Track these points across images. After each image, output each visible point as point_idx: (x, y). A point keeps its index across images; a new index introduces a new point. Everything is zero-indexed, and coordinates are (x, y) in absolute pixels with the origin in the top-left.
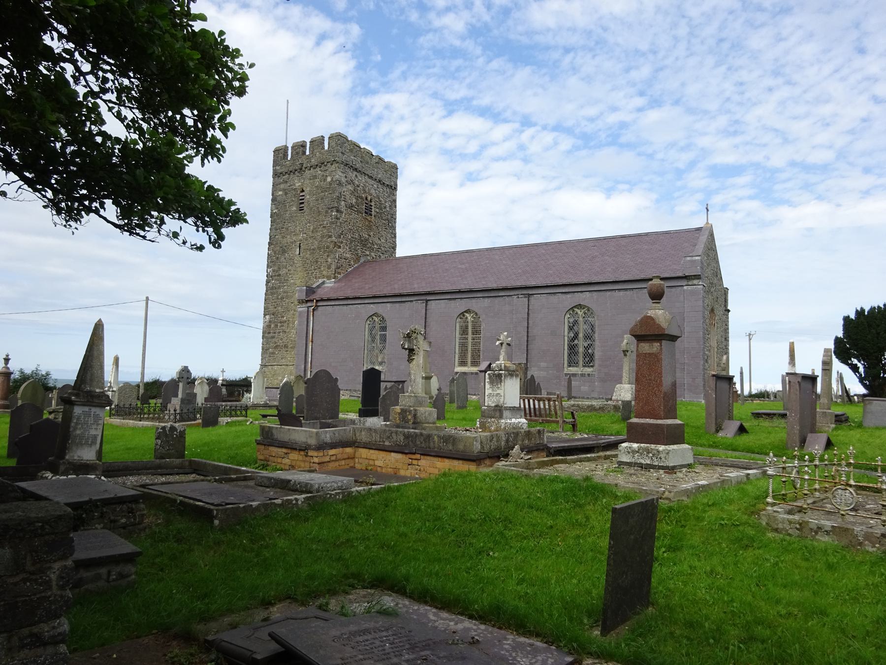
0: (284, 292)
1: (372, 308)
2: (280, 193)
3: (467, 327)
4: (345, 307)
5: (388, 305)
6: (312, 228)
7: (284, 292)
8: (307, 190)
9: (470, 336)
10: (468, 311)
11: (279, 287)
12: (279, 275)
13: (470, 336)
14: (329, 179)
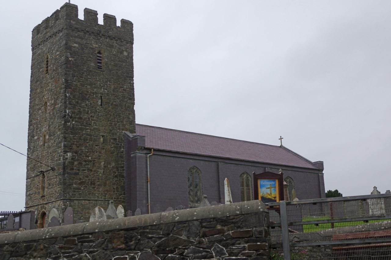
0: (88, 135)
1: (192, 163)
2: (75, 45)
3: (243, 182)
4: (172, 159)
5: (202, 162)
6: (113, 87)
7: (88, 135)
8: (105, 54)
9: (245, 188)
10: (243, 173)
11: (81, 129)
12: (81, 118)
13: (245, 188)
14: (125, 54)
